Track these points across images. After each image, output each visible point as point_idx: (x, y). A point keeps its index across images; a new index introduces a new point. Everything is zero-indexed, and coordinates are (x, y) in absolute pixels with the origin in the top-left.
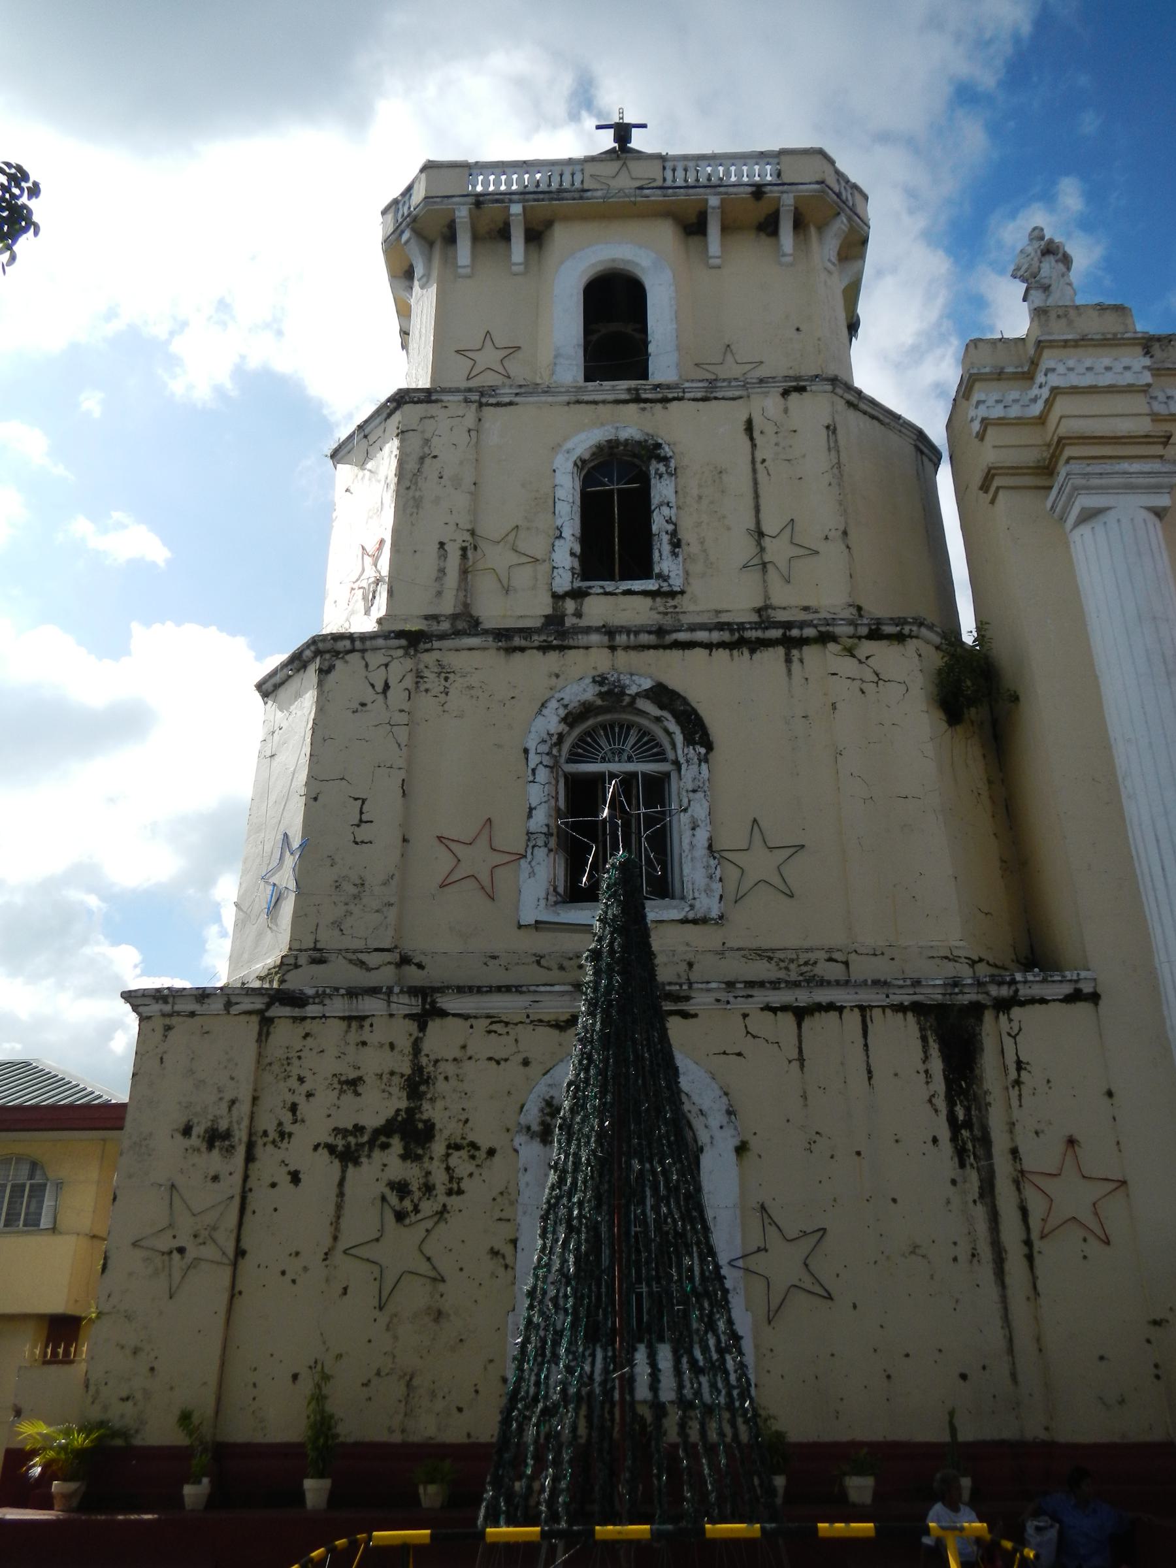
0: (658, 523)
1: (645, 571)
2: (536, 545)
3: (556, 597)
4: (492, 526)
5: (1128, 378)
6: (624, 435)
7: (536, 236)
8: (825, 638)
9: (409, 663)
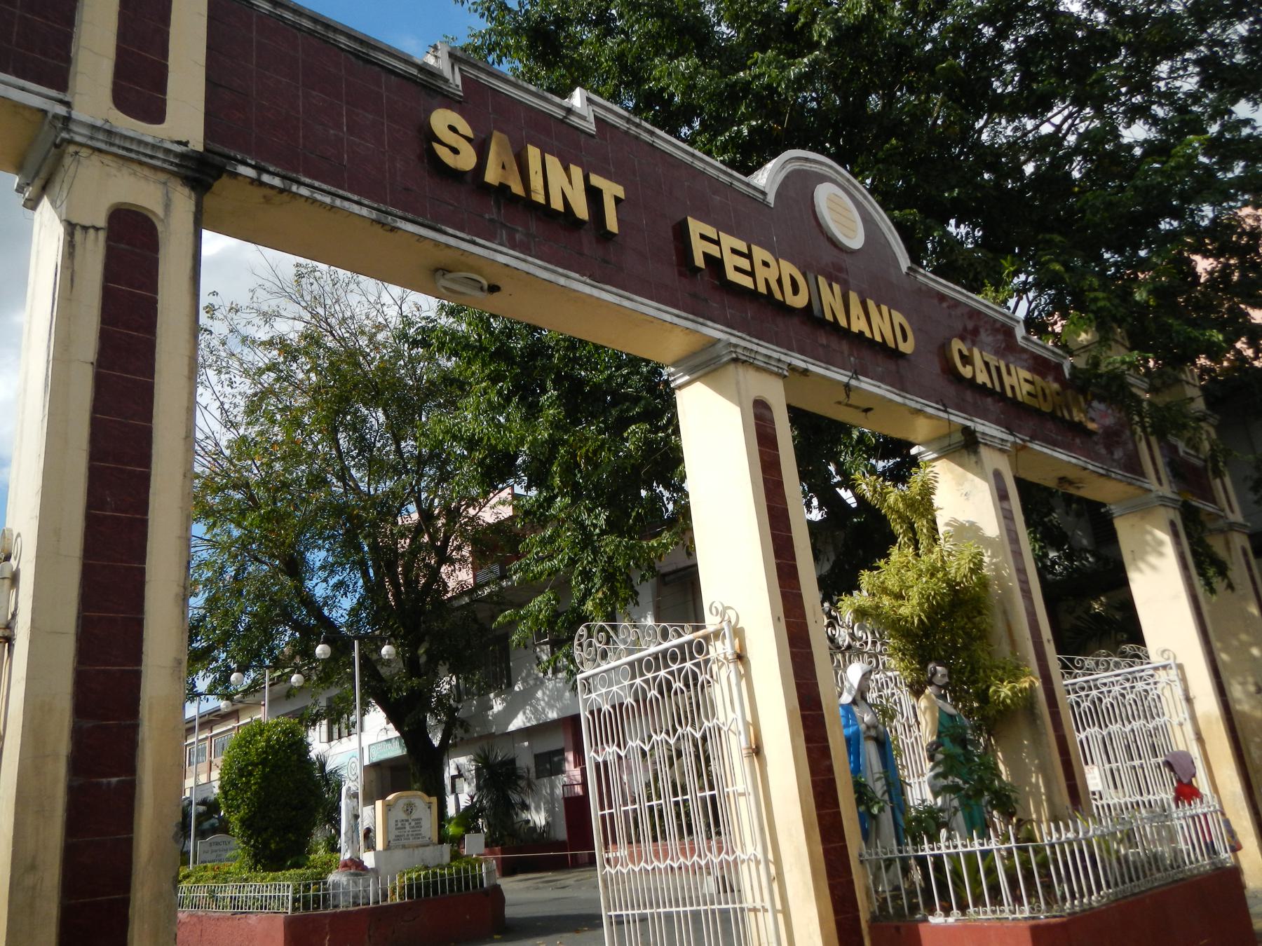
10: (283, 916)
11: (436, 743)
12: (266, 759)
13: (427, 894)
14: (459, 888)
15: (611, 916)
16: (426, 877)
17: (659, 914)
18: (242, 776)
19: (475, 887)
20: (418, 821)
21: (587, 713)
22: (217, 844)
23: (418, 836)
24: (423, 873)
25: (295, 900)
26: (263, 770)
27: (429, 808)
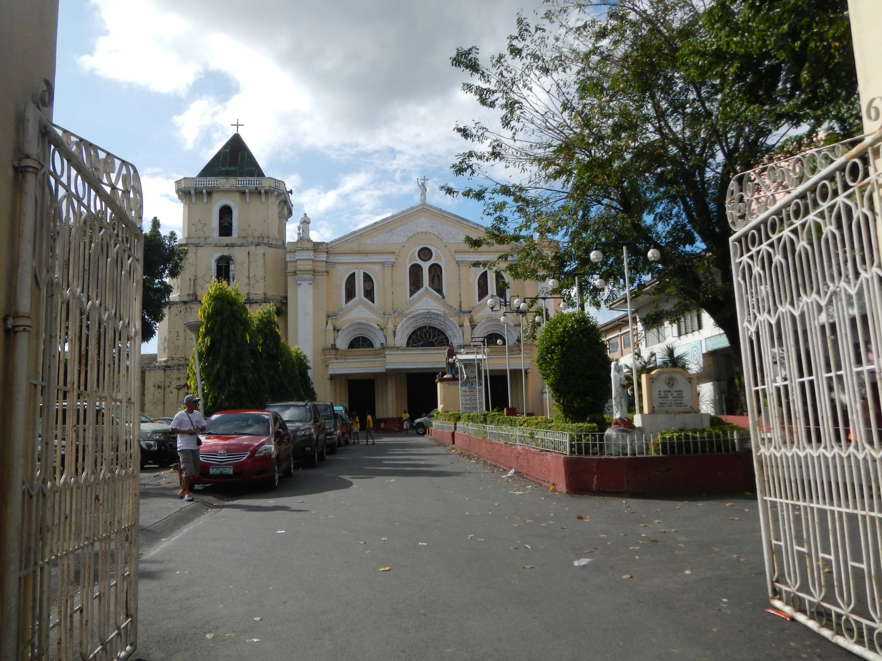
0: (231, 275)
4: (199, 275)
5: (310, 258)
6: (225, 254)
7: (209, 194)
8: (256, 303)
10: (562, 456)
12: (563, 341)
13: (680, 452)
14: (711, 450)
15: (766, 501)
16: (678, 438)
17: (812, 509)
18: (548, 353)
19: (727, 450)
20: (680, 392)
21: (740, 279)
23: (680, 405)
24: (675, 435)
25: (572, 446)
26: (562, 349)
27: (690, 382)
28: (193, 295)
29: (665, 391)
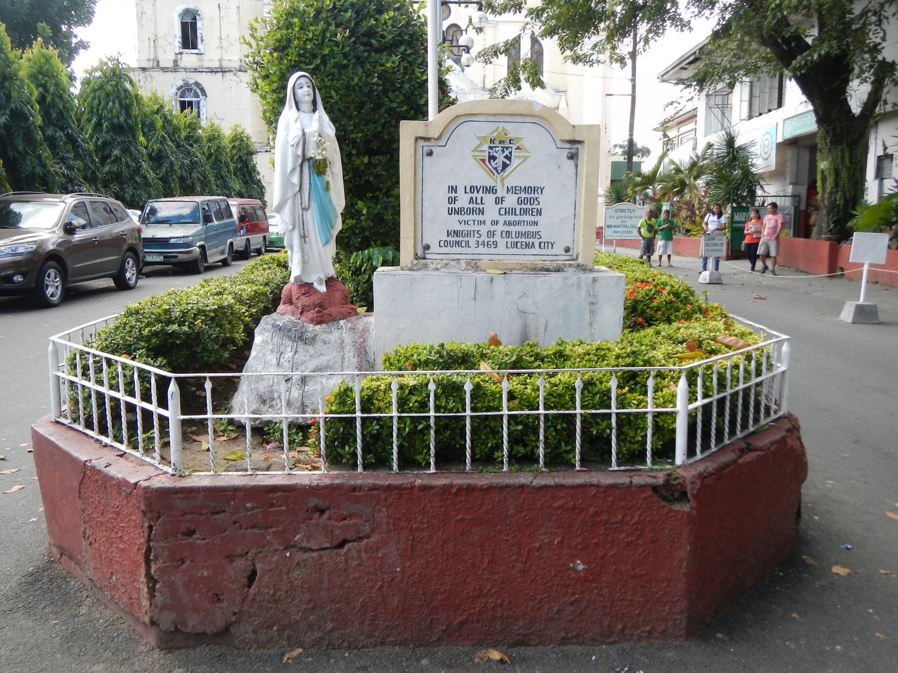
0: (198, 35)
1: (195, 47)
2: (170, 39)
3: (176, 54)
9: (143, 75)
11: (856, 107)
22: (622, 211)
27: (573, 157)
28: (153, 60)
29: (473, 189)
